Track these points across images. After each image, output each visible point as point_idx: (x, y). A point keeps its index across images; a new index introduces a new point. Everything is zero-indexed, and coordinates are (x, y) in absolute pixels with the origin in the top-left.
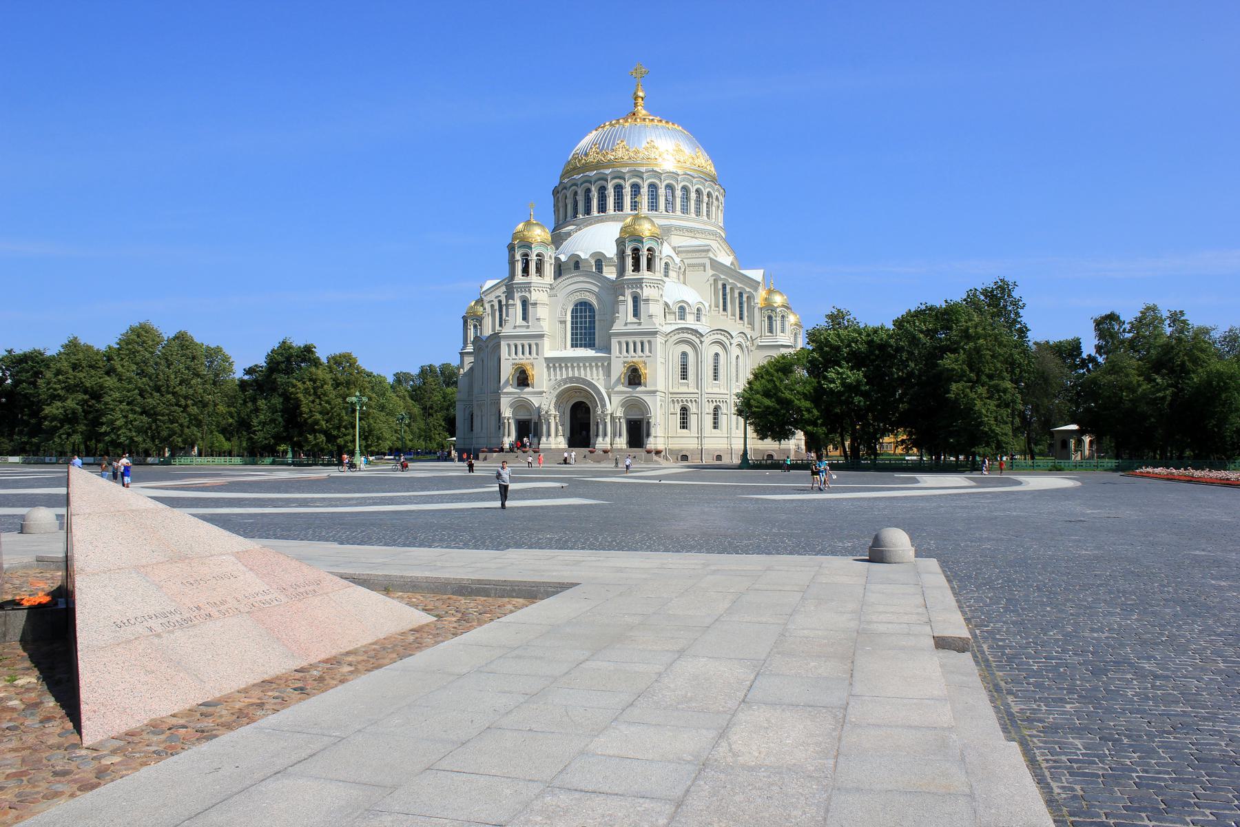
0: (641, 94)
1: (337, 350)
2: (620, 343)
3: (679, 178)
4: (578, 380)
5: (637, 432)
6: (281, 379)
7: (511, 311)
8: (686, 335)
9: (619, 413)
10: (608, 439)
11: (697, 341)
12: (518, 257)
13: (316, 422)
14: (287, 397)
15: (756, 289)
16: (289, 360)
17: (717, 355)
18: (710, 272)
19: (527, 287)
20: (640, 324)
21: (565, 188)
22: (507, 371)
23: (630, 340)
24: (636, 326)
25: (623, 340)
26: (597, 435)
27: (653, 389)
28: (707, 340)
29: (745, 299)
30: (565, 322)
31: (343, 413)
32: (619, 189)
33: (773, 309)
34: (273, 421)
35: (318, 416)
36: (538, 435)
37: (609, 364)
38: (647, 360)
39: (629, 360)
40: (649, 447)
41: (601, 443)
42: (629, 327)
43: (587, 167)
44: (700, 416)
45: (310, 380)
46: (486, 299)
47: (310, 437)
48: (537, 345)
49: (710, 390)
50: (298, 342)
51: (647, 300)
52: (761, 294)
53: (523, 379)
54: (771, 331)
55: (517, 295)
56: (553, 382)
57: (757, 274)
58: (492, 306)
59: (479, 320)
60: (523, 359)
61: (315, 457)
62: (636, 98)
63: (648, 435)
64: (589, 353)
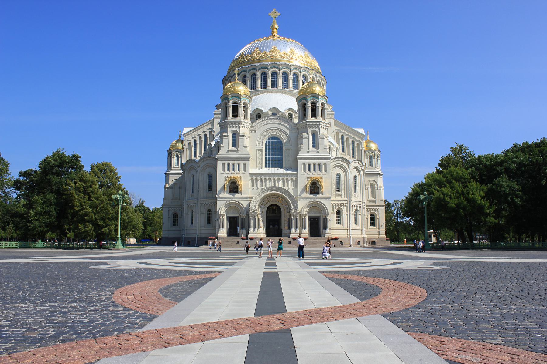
0: (276, 26)
1: (99, 160)
2: (304, 164)
3: (310, 72)
4: (277, 189)
5: (317, 226)
6: (55, 179)
7: (225, 140)
8: (340, 162)
9: (305, 213)
10: (298, 230)
11: (347, 166)
12: (230, 104)
13: (86, 214)
14: (59, 193)
15: (362, 139)
16: (59, 167)
17: (355, 176)
18: (334, 128)
19: (238, 124)
20: (318, 152)
21: (231, 77)
22: (222, 181)
23: (312, 162)
24: (315, 154)
25: (307, 162)
26: (290, 228)
27: (327, 196)
28: (352, 166)
29: (356, 145)
30: (262, 150)
31: (110, 208)
32: (275, 75)
33: (373, 152)
34: (48, 212)
35: (89, 210)
36: (246, 227)
37: (297, 179)
38: (323, 176)
39: (311, 176)
40: (327, 236)
41: (294, 233)
42: (310, 154)
43: (251, 61)
44: (348, 215)
45: (80, 181)
46: (185, 140)
47: (81, 226)
48: (244, 164)
49: (353, 199)
50: (69, 153)
51: (323, 136)
52: (364, 144)
53: (234, 187)
54: (371, 165)
55: (230, 130)
56: (260, 190)
57: (361, 131)
58: (190, 144)
59: (181, 152)
60: (235, 174)
61: (80, 240)
62: (273, 28)
63: (325, 228)
64: (282, 171)
